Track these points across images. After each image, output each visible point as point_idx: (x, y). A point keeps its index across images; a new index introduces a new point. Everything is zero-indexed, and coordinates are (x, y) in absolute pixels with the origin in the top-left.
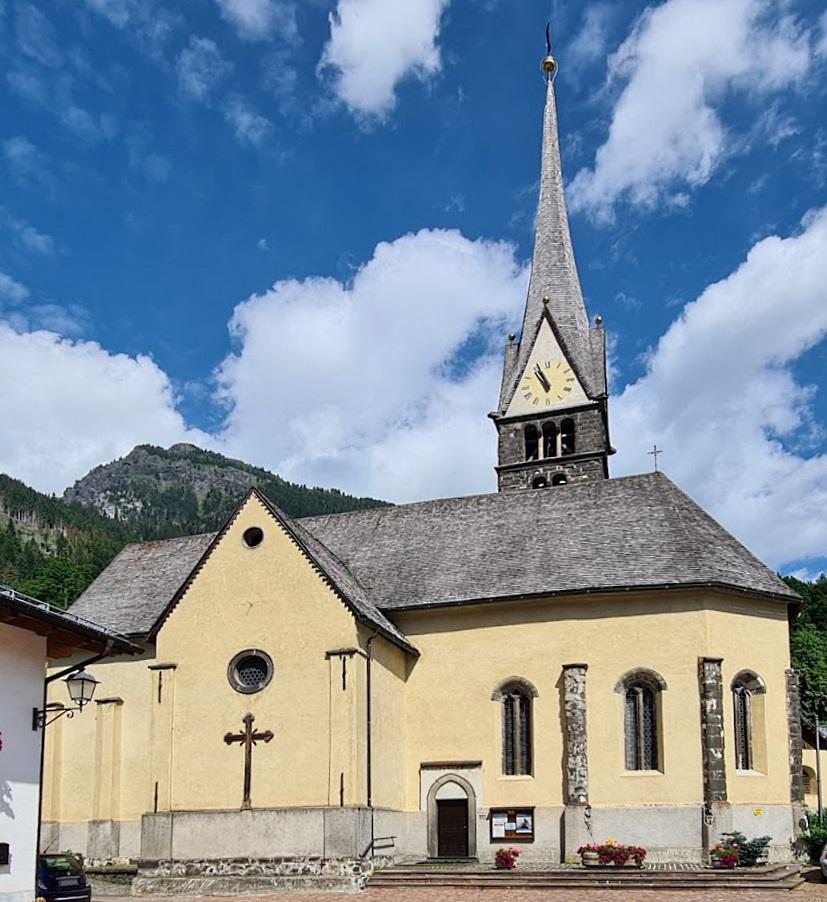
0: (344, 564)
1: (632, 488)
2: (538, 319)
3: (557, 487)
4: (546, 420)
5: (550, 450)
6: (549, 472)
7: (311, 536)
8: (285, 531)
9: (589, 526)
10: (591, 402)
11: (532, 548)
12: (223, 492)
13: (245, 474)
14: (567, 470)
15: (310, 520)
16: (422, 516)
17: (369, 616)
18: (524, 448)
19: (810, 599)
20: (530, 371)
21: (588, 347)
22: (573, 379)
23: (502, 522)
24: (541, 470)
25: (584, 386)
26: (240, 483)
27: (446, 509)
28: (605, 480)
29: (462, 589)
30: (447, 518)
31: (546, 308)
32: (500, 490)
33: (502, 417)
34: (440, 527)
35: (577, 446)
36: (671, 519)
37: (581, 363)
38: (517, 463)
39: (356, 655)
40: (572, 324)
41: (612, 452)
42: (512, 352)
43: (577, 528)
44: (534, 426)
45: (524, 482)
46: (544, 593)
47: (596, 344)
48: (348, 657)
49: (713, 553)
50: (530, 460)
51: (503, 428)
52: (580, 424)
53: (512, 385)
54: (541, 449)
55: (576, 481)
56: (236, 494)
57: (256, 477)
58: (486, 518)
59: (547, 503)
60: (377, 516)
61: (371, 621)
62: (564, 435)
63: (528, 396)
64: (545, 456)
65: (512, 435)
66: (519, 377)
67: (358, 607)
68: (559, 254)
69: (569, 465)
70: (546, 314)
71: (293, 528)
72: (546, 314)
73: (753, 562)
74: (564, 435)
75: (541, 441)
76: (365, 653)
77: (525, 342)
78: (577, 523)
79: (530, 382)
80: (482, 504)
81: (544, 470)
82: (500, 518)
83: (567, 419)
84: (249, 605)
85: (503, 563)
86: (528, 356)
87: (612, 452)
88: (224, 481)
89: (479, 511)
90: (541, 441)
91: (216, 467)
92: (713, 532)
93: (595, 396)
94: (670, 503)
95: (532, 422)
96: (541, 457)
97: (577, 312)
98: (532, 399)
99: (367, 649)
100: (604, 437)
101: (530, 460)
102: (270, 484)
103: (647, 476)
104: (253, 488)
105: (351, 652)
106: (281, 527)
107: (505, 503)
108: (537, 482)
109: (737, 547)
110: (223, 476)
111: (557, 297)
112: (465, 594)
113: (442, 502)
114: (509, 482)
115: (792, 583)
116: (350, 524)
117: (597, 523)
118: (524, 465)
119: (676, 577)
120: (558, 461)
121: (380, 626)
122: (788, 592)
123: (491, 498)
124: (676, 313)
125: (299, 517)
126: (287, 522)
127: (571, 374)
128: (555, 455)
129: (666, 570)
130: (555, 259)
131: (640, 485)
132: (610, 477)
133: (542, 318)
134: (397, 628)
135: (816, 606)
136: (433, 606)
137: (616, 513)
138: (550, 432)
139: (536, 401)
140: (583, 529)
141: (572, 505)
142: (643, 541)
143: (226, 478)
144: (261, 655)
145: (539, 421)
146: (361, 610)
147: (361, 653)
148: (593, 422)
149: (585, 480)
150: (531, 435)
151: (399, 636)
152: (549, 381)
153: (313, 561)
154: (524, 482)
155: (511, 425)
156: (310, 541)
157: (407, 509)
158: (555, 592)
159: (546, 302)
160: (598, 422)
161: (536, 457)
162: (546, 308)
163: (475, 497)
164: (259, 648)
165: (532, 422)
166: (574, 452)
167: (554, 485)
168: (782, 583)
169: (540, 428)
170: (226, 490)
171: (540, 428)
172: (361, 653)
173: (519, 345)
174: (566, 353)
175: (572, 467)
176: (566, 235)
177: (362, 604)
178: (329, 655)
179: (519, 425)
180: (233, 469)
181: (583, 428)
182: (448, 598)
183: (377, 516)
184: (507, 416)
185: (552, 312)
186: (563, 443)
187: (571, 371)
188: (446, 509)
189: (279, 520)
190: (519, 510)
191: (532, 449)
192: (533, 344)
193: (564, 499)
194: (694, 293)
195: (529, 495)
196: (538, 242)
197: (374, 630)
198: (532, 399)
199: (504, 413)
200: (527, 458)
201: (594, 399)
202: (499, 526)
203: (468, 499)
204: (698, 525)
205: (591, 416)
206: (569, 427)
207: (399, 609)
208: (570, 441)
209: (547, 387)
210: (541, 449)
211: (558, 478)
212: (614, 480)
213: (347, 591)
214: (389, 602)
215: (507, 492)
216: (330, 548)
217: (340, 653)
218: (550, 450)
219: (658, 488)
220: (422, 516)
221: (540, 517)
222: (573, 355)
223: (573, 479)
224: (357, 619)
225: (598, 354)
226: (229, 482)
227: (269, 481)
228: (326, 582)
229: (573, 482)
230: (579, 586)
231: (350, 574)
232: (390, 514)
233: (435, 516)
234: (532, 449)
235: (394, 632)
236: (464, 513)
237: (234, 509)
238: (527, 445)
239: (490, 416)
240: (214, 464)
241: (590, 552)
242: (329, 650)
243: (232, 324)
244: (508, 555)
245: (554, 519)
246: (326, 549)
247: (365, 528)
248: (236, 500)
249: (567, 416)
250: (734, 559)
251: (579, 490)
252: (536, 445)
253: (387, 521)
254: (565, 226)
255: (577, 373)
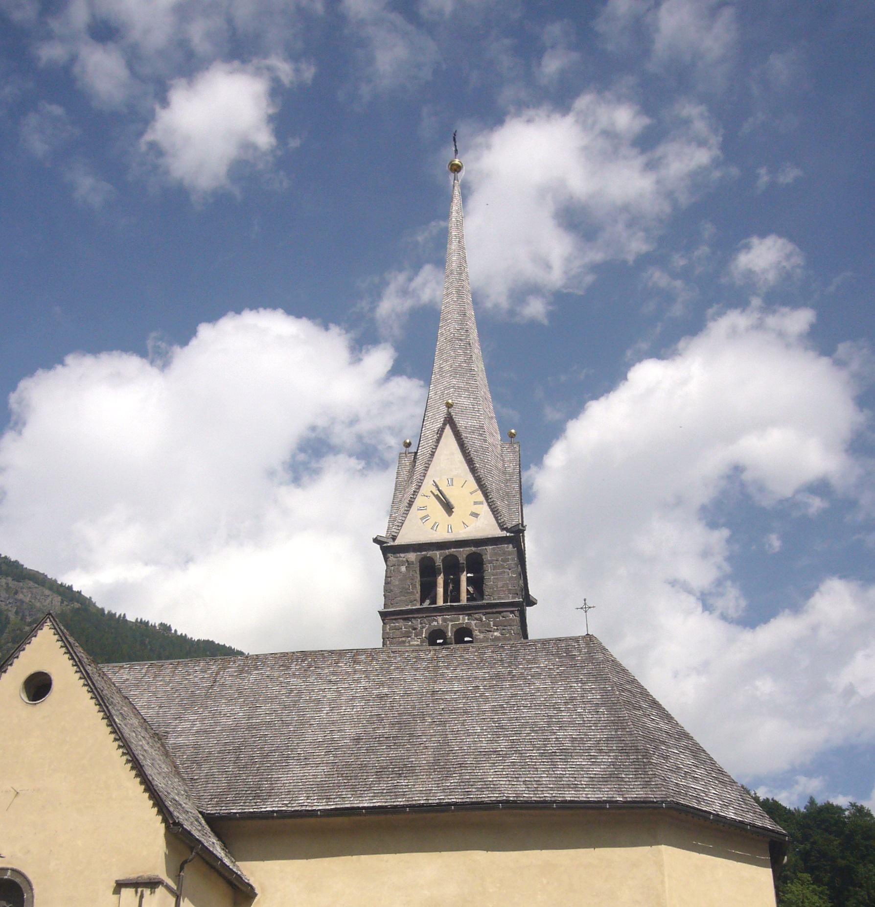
0: (159, 738)
1: (558, 655)
2: (439, 425)
3: (462, 645)
4: (447, 552)
5: (453, 594)
6: (450, 624)
7: (119, 691)
8: (82, 681)
9: (502, 706)
10: (504, 534)
11: (424, 734)
12: (12, 616)
13: (47, 592)
14: (473, 622)
15: (122, 667)
16: (276, 674)
17: (187, 826)
18: (418, 587)
19: (799, 835)
20: (427, 487)
21: (500, 465)
22: (481, 503)
23: (386, 690)
24: (440, 619)
25: (495, 511)
26: (38, 604)
27: (310, 666)
28: (525, 641)
29: (322, 788)
30: (311, 679)
31: (449, 414)
32: (384, 644)
33: (392, 544)
34: (300, 693)
35: (487, 591)
36: (608, 701)
37: (492, 483)
38: (409, 607)
39: (160, 890)
40: (481, 435)
41: (531, 602)
42: (407, 461)
43: (487, 707)
44: (431, 560)
45: (416, 636)
46: (439, 805)
47: (510, 461)
48: (147, 892)
49: (666, 758)
50: (426, 604)
51: (392, 558)
52: (491, 562)
53: (405, 503)
54: (440, 590)
55: (486, 640)
56: (29, 619)
57: (59, 598)
58: (364, 683)
59: (447, 669)
60: (214, 668)
61: (189, 833)
62: (469, 575)
63: (425, 518)
64: (445, 601)
65: (403, 569)
66: (415, 493)
67: (171, 809)
68: (465, 354)
69: (477, 616)
70: (450, 420)
71: (96, 677)
72: (450, 420)
73: (720, 776)
74: (469, 575)
75: (440, 580)
76: (175, 888)
77: (424, 453)
78: (487, 700)
79: (426, 501)
80: (359, 663)
81: (445, 620)
82: (382, 684)
83: (475, 553)
84: (13, 793)
85: (384, 755)
86: (427, 468)
87: (531, 602)
88: (16, 600)
89: (355, 672)
90: (440, 580)
91: (10, 579)
92: (665, 727)
93: (509, 526)
94: (606, 679)
95: (430, 554)
96: (440, 602)
97: (487, 421)
98: (429, 524)
99: (178, 879)
100: (521, 582)
101: (426, 604)
102: (78, 609)
103: (576, 639)
104: (50, 614)
105: (153, 884)
106: (78, 675)
107: (391, 665)
108: (435, 637)
109: (697, 751)
110: (16, 593)
111: (463, 401)
112: (328, 799)
113: (305, 654)
114: (398, 633)
115: (771, 808)
116: (177, 678)
117: (513, 702)
118: (418, 611)
119: (619, 791)
120: (462, 609)
121: (200, 842)
122: (768, 824)
123: (372, 654)
124: (556, 432)
125: (108, 661)
126: (88, 668)
127: (480, 496)
128: (459, 601)
129: (606, 779)
130: (461, 359)
131: (567, 651)
132: (530, 637)
133: (444, 424)
134: (226, 846)
135: (808, 847)
136: (282, 815)
137: (538, 690)
138: (452, 568)
139: (435, 526)
140: (494, 710)
141: (480, 673)
142: (575, 734)
143: (20, 596)
144: (18, 880)
145: (438, 553)
146: (176, 814)
147: (168, 887)
148: (508, 560)
149: (497, 639)
150: (428, 570)
151: (227, 861)
152: (452, 501)
153: (116, 730)
154: (416, 636)
155: (402, 555)
156: (117, 699)
157: (258, 661)
158: (455, 804)
159: (449, 406)
160: (513, 560)
161: (434, 601)
162: (449, 414)
163: (351, 651)
164: (15, 867)
165: (430, 554)
166: (483, 599)
167: (456, 643)
168: (759, 809)
169: (439, 562)
170: (17, 613)
171: (439, 562)
172: (168, 887)
173: (416, 453)
174: (473, 470)
175: (481, 620)
176: (474, 334)
177: (177, 804)
178: (120, 886)
179: (412, 556)
180: (31, 584)
181: (495, 568)
182: (304, 802)
183: (214, 668)
184: (397, 542)
185: (456, 419)
186: (468, 585)
187: (479, 492)
188: (310, 666)
189: (78, 664)
190: (408, 675)
191: (428, 591)
192: (433, 454)
193: (469, 664)
194: (576, 411)
195: (422, 655)
196: (441, 339)
197: (192, 849)
198: (429, 524)
199: (394, 538)
200: (422, 601)
201: (507, 530)
202: (381, 697)
203: (341, 653)
204: (645, 715)
205: (504, 553)
206: (476, 564)
207: (230, 817)
208: (477, 583)
209: (448, 508)
210: (440, 590)
211: (462, 634)
212: (536, 642)
213: (159, 782)
214: (217, 804)
215: (394, 648)
216: (143, 712)
217: (136, 884)
218: (453, 594)
219: (591, 659)
220: (276, 674)
221: (437, 688)
222: (482, 473)
223: (481, 636)
224: (167, 828)
225: (511, 475)
226: (22, 602)
227: (77, 605)
228: (130, 765)
229: (482, 641)
230: (488, 796)
231: (166, 754)
232: (232, 669)
233: (294, 675)
234: (428, 591)
235: (219, 850)
236: (334, 673)
237: (21, 640)
238: (422, 585)
239: (376, 541)
240: (7, 575)
241: (503, 745)
242: (121, 876)
243: (13, 398)
244: (391, 742)
245: (455, 692)
246: (137, 713)
247: (196, 684)
248: (27, 628)
249: (473, 549)
250: (694, 768)
251: (489, 653)
252: (434, 585)
253: (228, 677)
254: (472, 325)
255: (486, 495)
